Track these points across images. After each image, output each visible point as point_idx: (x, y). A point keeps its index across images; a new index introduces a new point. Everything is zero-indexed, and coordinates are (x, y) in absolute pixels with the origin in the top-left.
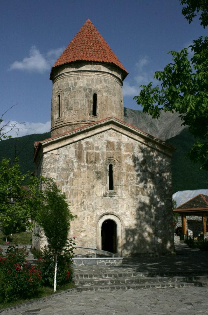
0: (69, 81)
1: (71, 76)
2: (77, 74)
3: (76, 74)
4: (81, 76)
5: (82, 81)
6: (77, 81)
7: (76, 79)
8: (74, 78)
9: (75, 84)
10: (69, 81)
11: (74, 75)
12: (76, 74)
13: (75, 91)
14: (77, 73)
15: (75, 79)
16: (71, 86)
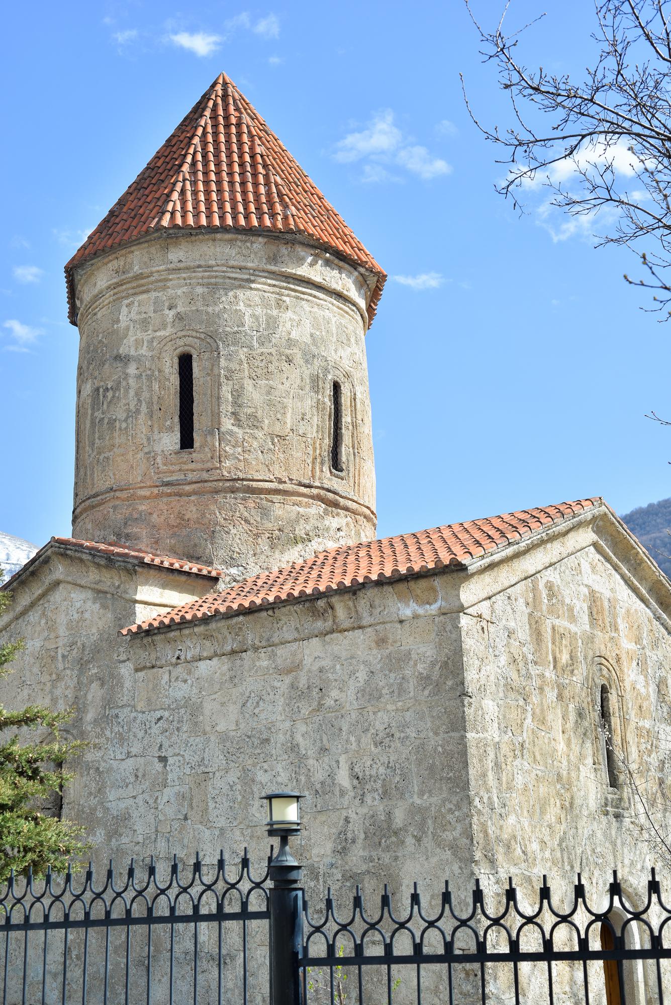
0: (241, 304)
1: (251, 289)
2: (274, 286)
3: (270, 285)
4: (288, 295)
5: (296, 318)
6: (275, 312)
7: (273, 303)
8: (262, 298)
9: (268, 324)
10: (241, 304)
11: (263, 287)
12: (270, 285)
13: (271, 354)
14: (274, 282)
15: (266, 305)
16: (251, 329)
